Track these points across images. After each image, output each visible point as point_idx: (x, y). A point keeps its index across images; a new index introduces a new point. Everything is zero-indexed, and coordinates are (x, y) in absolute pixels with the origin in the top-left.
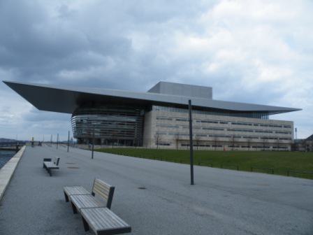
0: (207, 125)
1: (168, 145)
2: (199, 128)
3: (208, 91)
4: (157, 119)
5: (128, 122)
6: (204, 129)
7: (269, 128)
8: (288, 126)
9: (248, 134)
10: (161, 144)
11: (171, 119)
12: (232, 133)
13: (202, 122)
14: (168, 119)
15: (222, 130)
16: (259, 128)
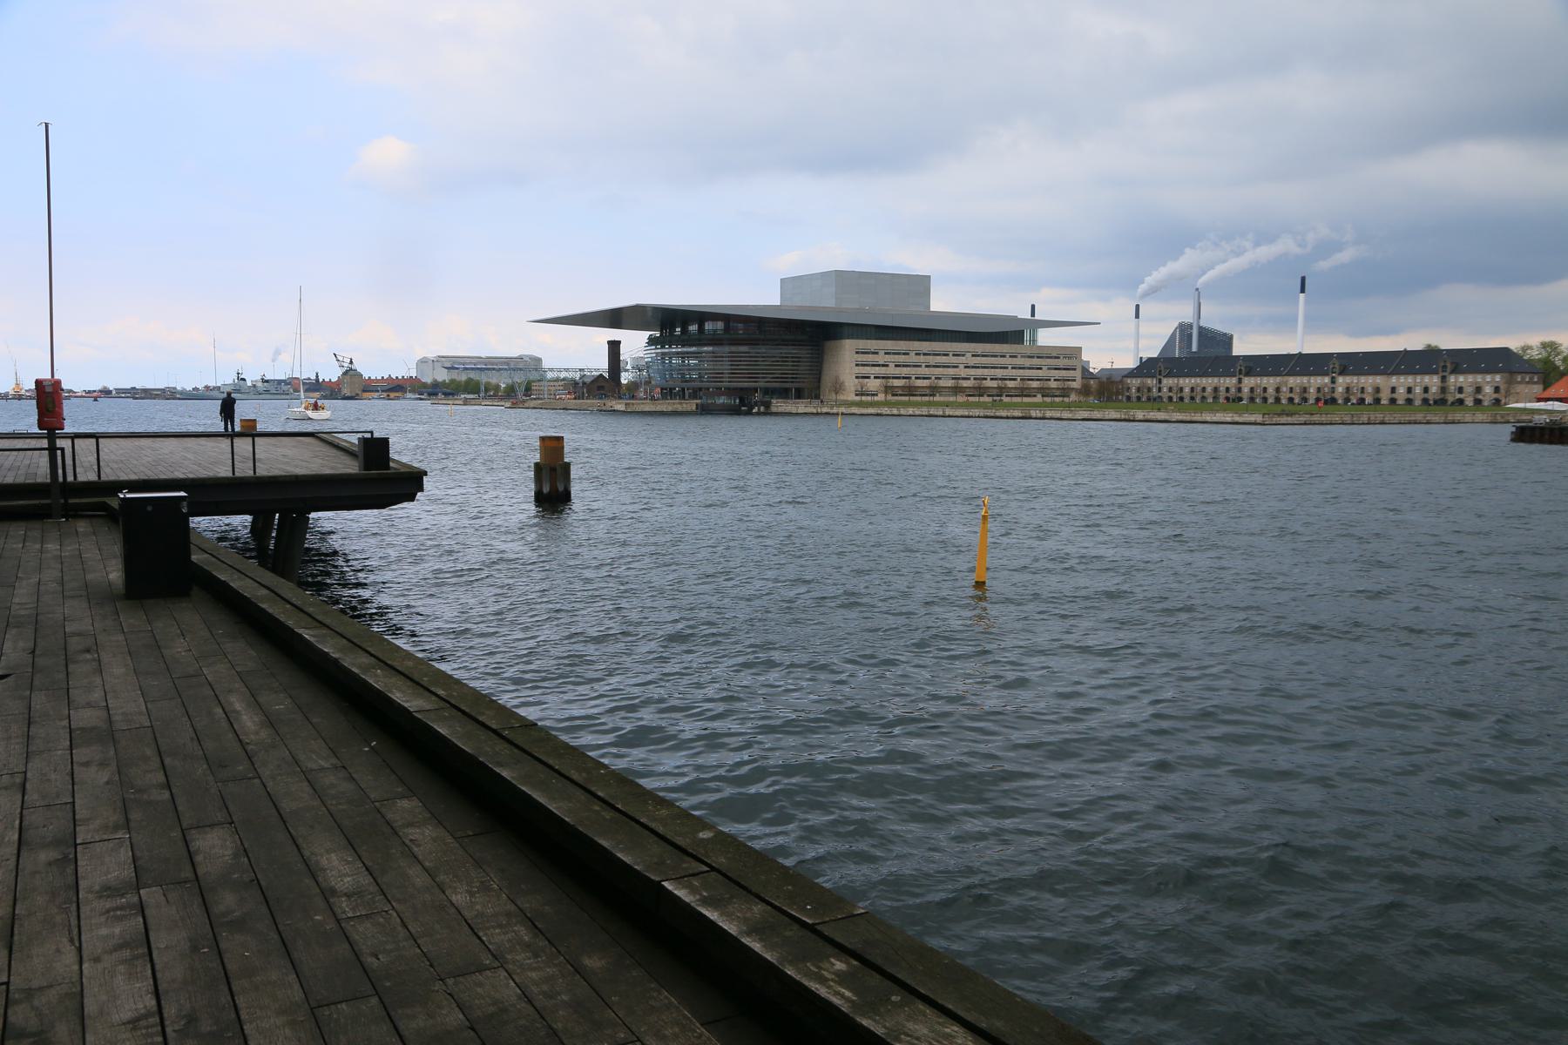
0: (932, 360)
1: (873, 395)
2: (920, 366)
3: (920, 285)
4: (857, 353)
5: (722, 344)
6: (927, 366)
7: (1036, 362)
8: (1075, 353)
9: (999, 373)
10: (868, 395)
11: (877, 353)
12: (972, 372)
13: (924, 354)
14: (874, 353)
15: (957, 367)
16: (1019, 361)
